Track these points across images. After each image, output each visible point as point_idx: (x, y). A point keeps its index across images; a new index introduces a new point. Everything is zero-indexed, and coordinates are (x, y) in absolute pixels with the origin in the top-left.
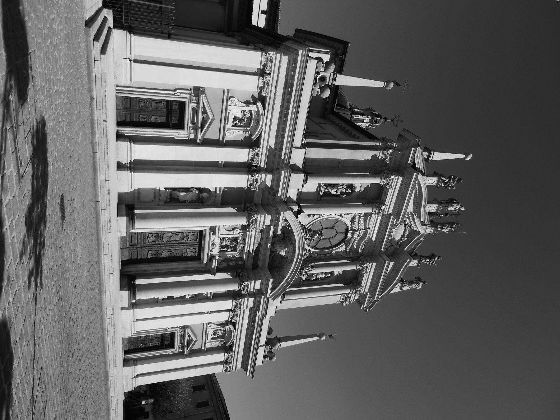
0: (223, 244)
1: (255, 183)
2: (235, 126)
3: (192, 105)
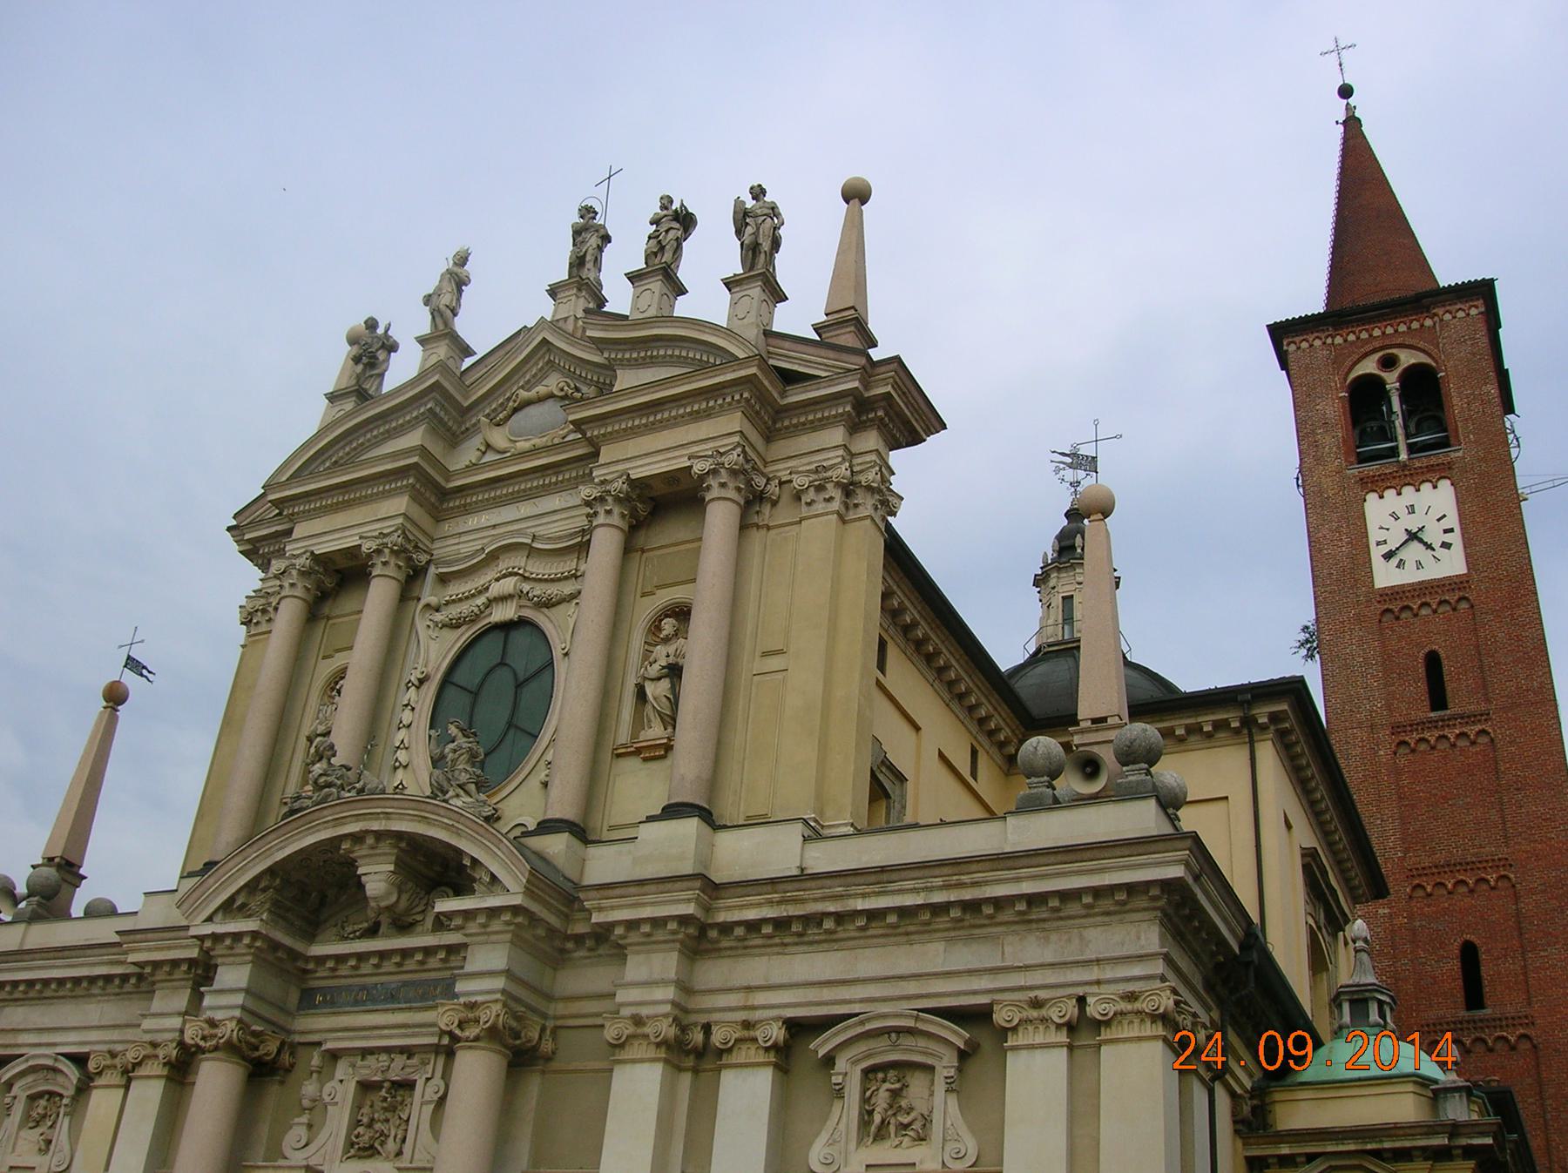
2: (49, 1142)
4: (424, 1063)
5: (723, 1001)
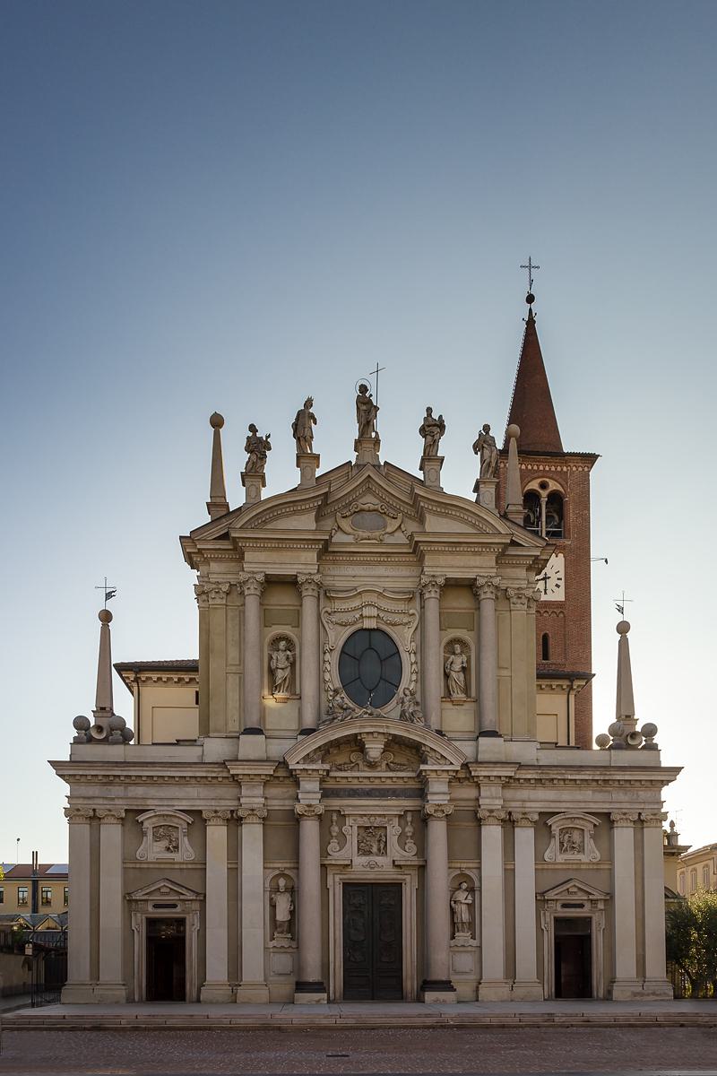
0: (375, 850)
1: (255, 812)
2: (176, 847)
3: (150, 909)
4: (389, 820)
5: (513, 804)
